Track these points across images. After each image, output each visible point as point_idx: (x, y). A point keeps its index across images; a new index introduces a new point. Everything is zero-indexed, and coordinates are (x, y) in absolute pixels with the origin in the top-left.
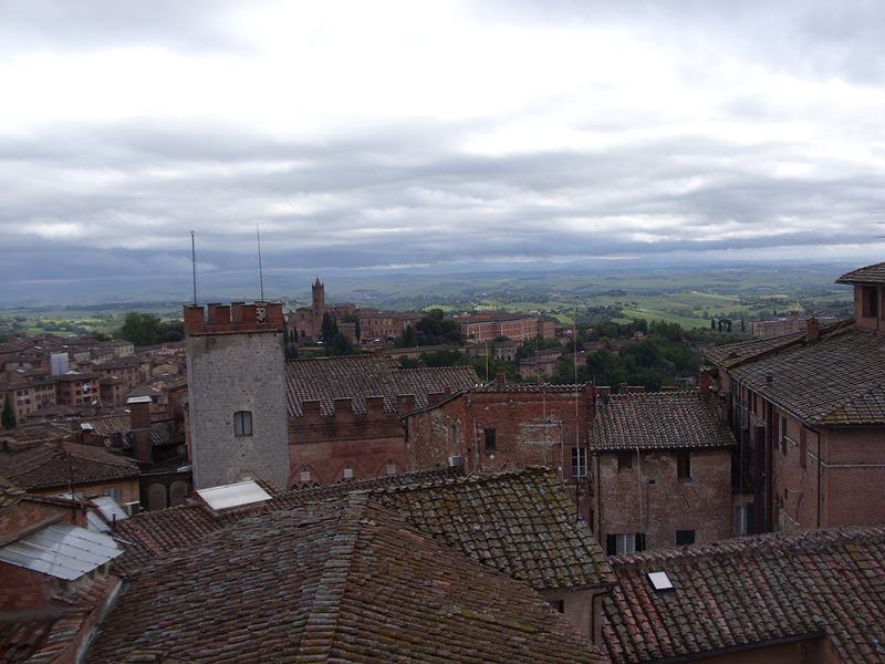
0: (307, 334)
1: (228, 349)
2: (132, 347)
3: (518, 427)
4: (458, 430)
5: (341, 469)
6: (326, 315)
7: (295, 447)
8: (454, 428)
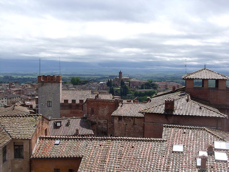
1: (47, 86)
3: (99, 109)
6: (122, 80)
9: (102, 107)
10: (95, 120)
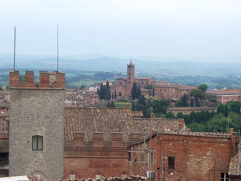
1: (32, 98)
4: (154, 156)
7: (67, 160)
8: (152, 154)
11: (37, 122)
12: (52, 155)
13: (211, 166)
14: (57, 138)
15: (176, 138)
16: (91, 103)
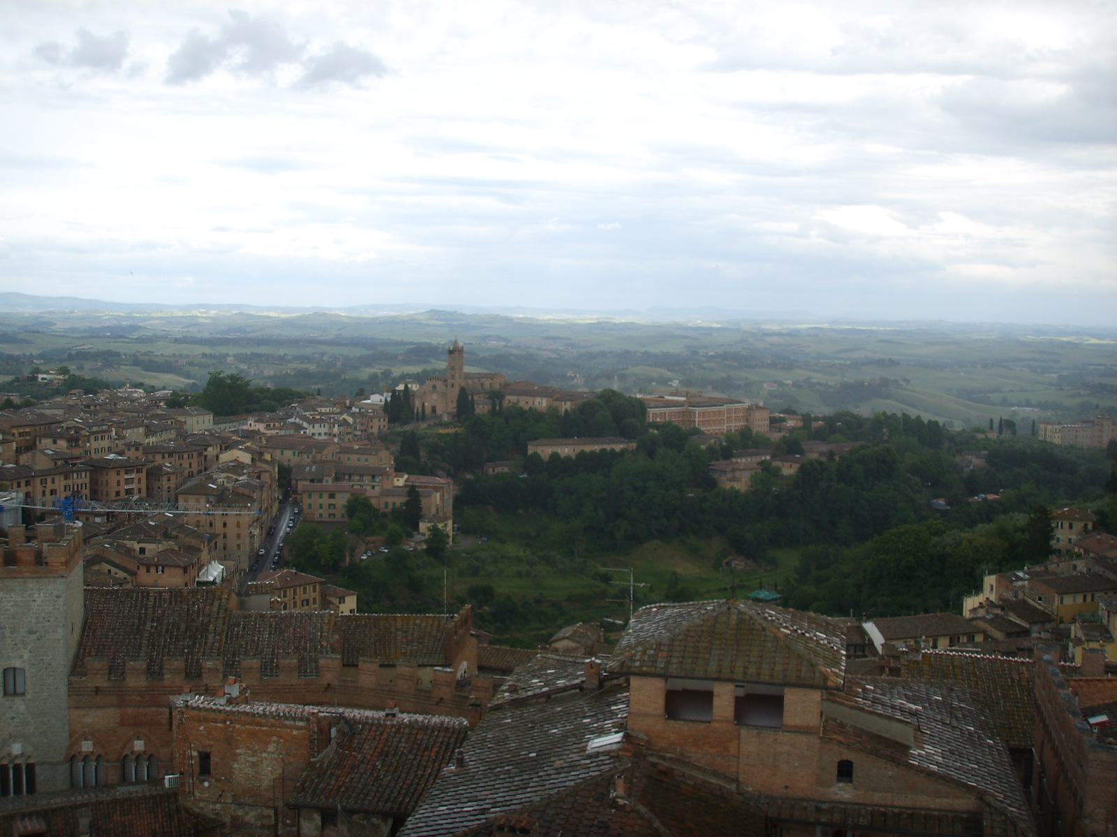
0: (439, 412)
2: (211, 417)
5: (130, 741)
7: (77, 712)
9: (248, 748)
10: (218, 806)
11: (12, 641)
12: (44, 703)
13: (277, 772)
14: (53, 671)
15: (212, 715)
16: (370, 431)
